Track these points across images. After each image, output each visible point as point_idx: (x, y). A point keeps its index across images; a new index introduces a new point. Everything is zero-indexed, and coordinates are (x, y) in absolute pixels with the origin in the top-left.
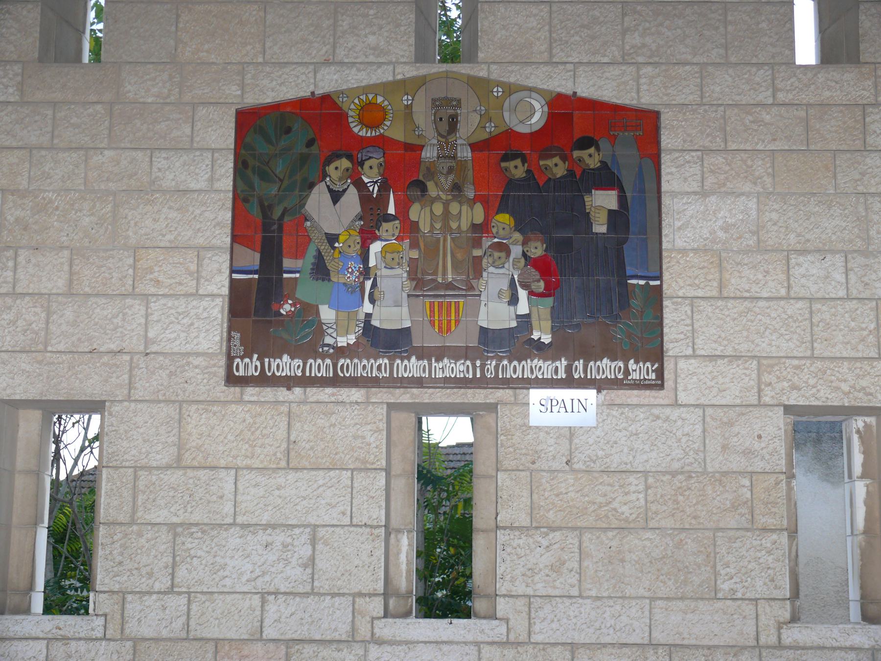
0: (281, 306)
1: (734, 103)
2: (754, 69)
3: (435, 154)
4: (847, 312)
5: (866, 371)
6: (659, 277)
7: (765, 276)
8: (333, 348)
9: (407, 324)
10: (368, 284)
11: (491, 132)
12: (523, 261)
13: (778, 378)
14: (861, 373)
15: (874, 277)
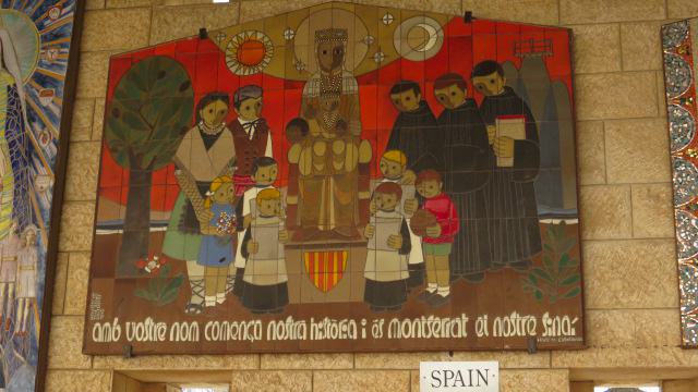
0: (146, 264)
3: (318, 90)
6: (579, 215)
8: (201, 309)
9: (283, 279)
10: (241, 236)
11: (379, 63)
12: (416, 203)
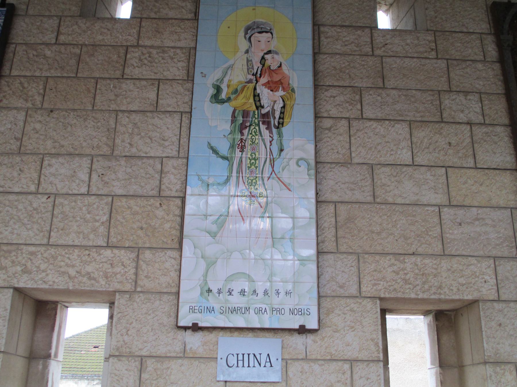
1: (24, 42)
2: (45, 19)
4: (85, 206)
5: (93, 258)
7: (19, 175)
13: (13, 262)
14: (89, 259)
15: (113, 176)
